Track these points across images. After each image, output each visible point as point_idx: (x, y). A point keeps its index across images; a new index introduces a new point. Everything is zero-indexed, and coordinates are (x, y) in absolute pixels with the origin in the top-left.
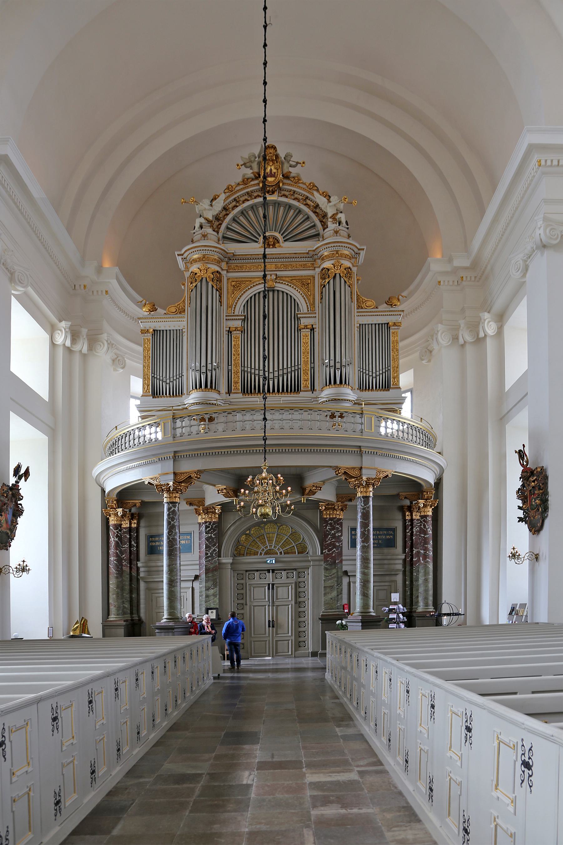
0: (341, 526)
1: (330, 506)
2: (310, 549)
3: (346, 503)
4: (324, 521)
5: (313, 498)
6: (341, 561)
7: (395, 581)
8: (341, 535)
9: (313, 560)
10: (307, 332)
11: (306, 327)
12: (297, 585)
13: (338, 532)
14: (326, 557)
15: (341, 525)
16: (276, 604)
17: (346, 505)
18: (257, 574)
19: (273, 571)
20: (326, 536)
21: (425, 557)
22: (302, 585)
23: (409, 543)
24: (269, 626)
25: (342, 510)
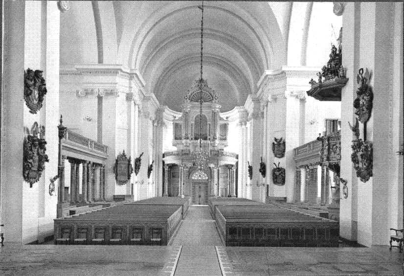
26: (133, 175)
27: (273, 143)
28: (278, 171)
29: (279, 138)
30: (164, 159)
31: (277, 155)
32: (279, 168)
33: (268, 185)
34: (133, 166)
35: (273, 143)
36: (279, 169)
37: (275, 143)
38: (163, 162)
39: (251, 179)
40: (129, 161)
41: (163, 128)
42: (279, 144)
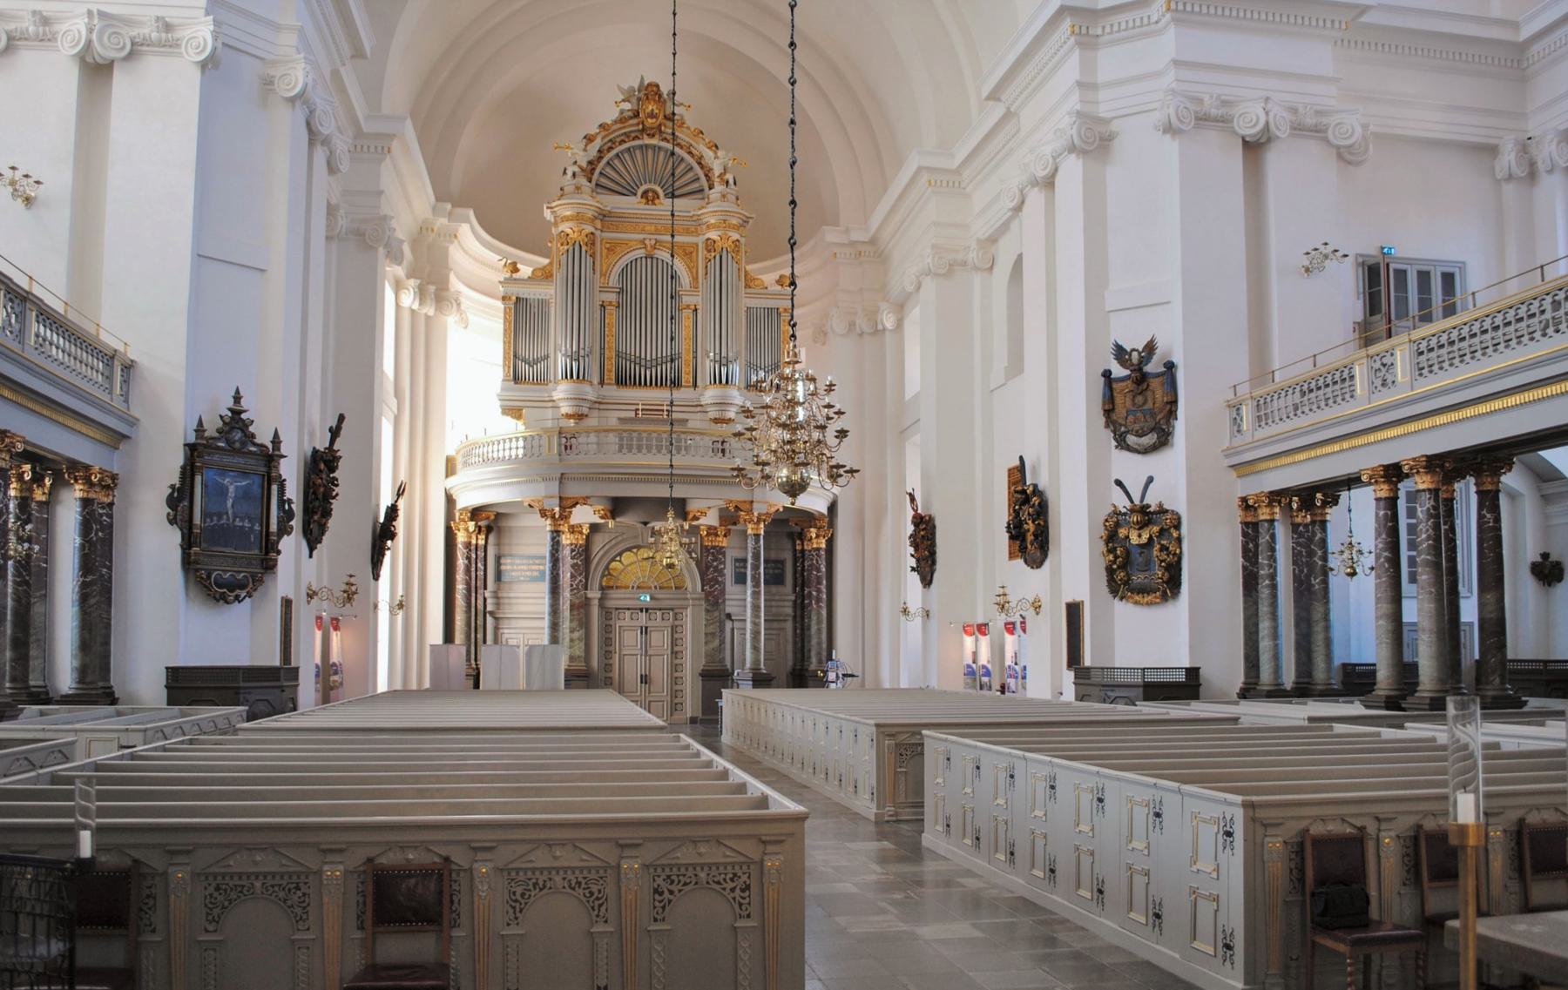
0: (724, 556)
1: (712, 531)
2: (688, 584)
3: (729, 527)
4: (705, 549)
5: (695, 523)
6: (724, 602)
7: (783, 629)
8: (724, 568)
9: (693, 599)
10: (687, 313)
11: (688, 307)
12: (674, 629)
13: (721, 563)
14: (708, 594)
15: (724, 554)
16: (650, 652)
17: (729, 530)
18: (628, 613)
19: (647, 610)
20: (707, 568)
21: (819, 600)
22: (679, 629)
23: (799, 581)
24: (642, 682)
25: (725, 536)
26: (291, 546)
27: (1107, 374)
28: (1142, 526)
29: (1134, 342)
30: (451, 482)
31: (1131, 439)
32: (1143, 510)
33: (1074, 611)
34: (293, 491)
35: (1107, 374)
36: (1145, 515)
37: (1118, 371)
38: (450, 501)
39: (927, 581)
40: (270, 457)
41: (451, 320)
42: (1140, 378)
